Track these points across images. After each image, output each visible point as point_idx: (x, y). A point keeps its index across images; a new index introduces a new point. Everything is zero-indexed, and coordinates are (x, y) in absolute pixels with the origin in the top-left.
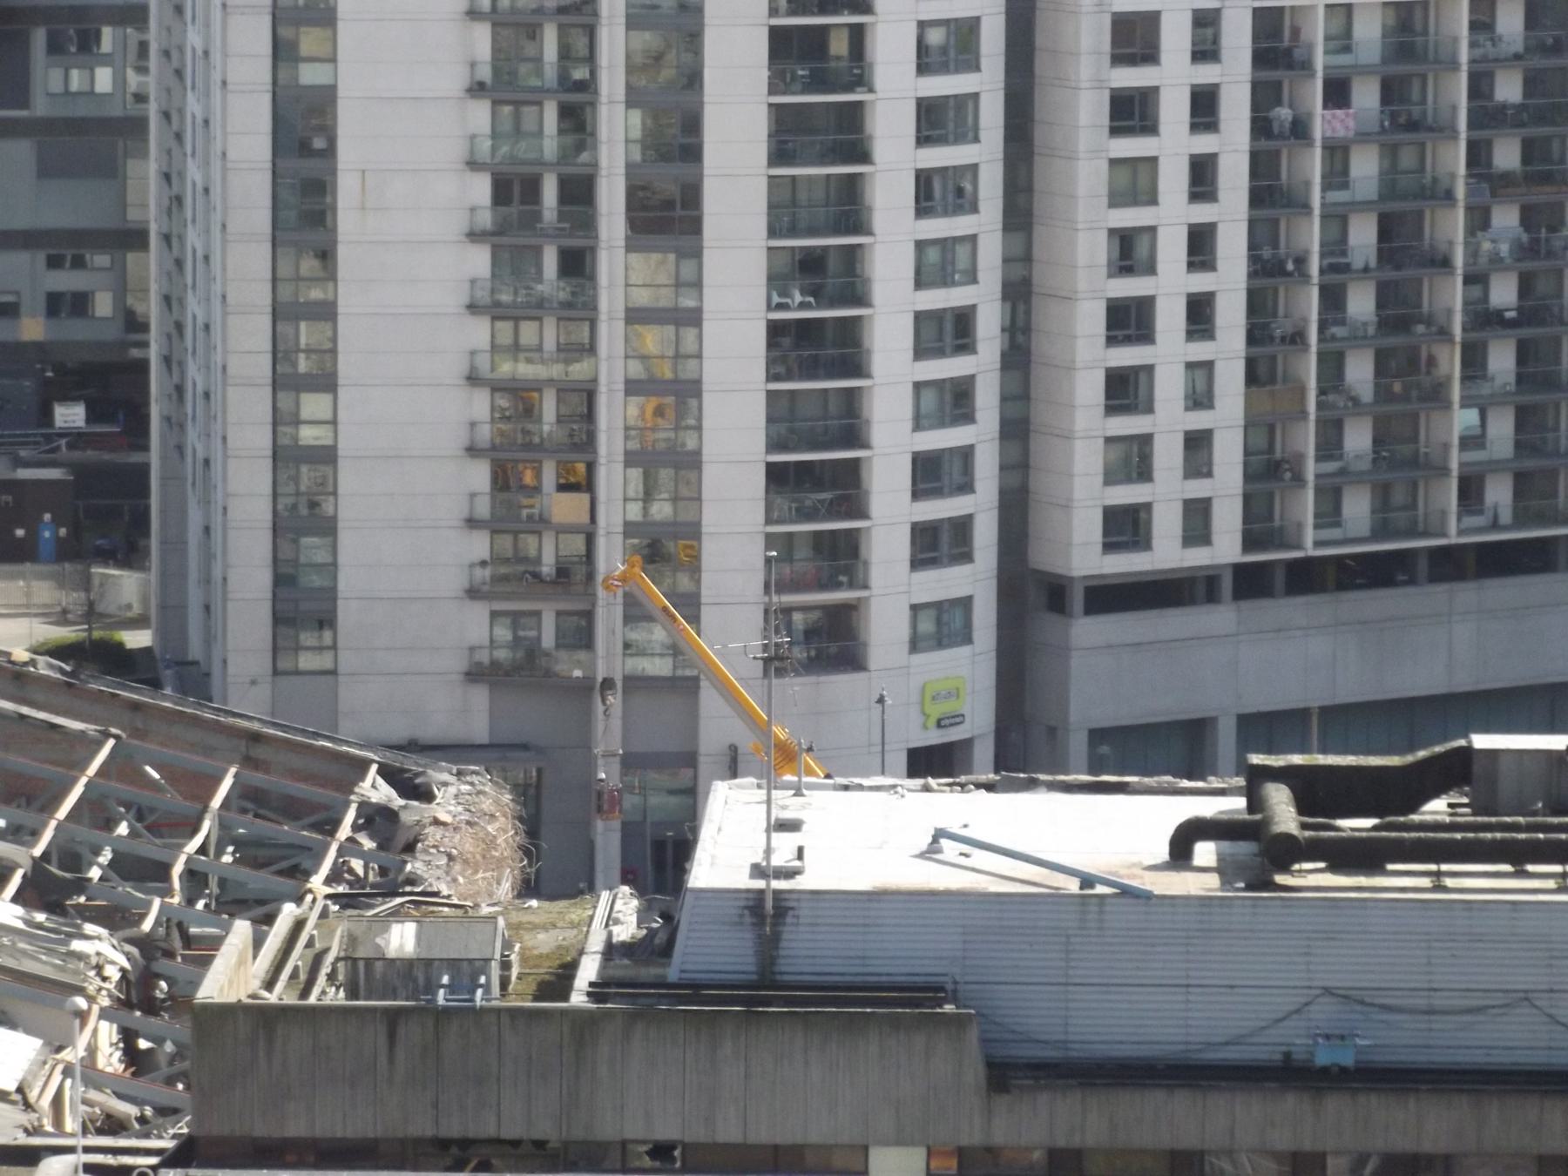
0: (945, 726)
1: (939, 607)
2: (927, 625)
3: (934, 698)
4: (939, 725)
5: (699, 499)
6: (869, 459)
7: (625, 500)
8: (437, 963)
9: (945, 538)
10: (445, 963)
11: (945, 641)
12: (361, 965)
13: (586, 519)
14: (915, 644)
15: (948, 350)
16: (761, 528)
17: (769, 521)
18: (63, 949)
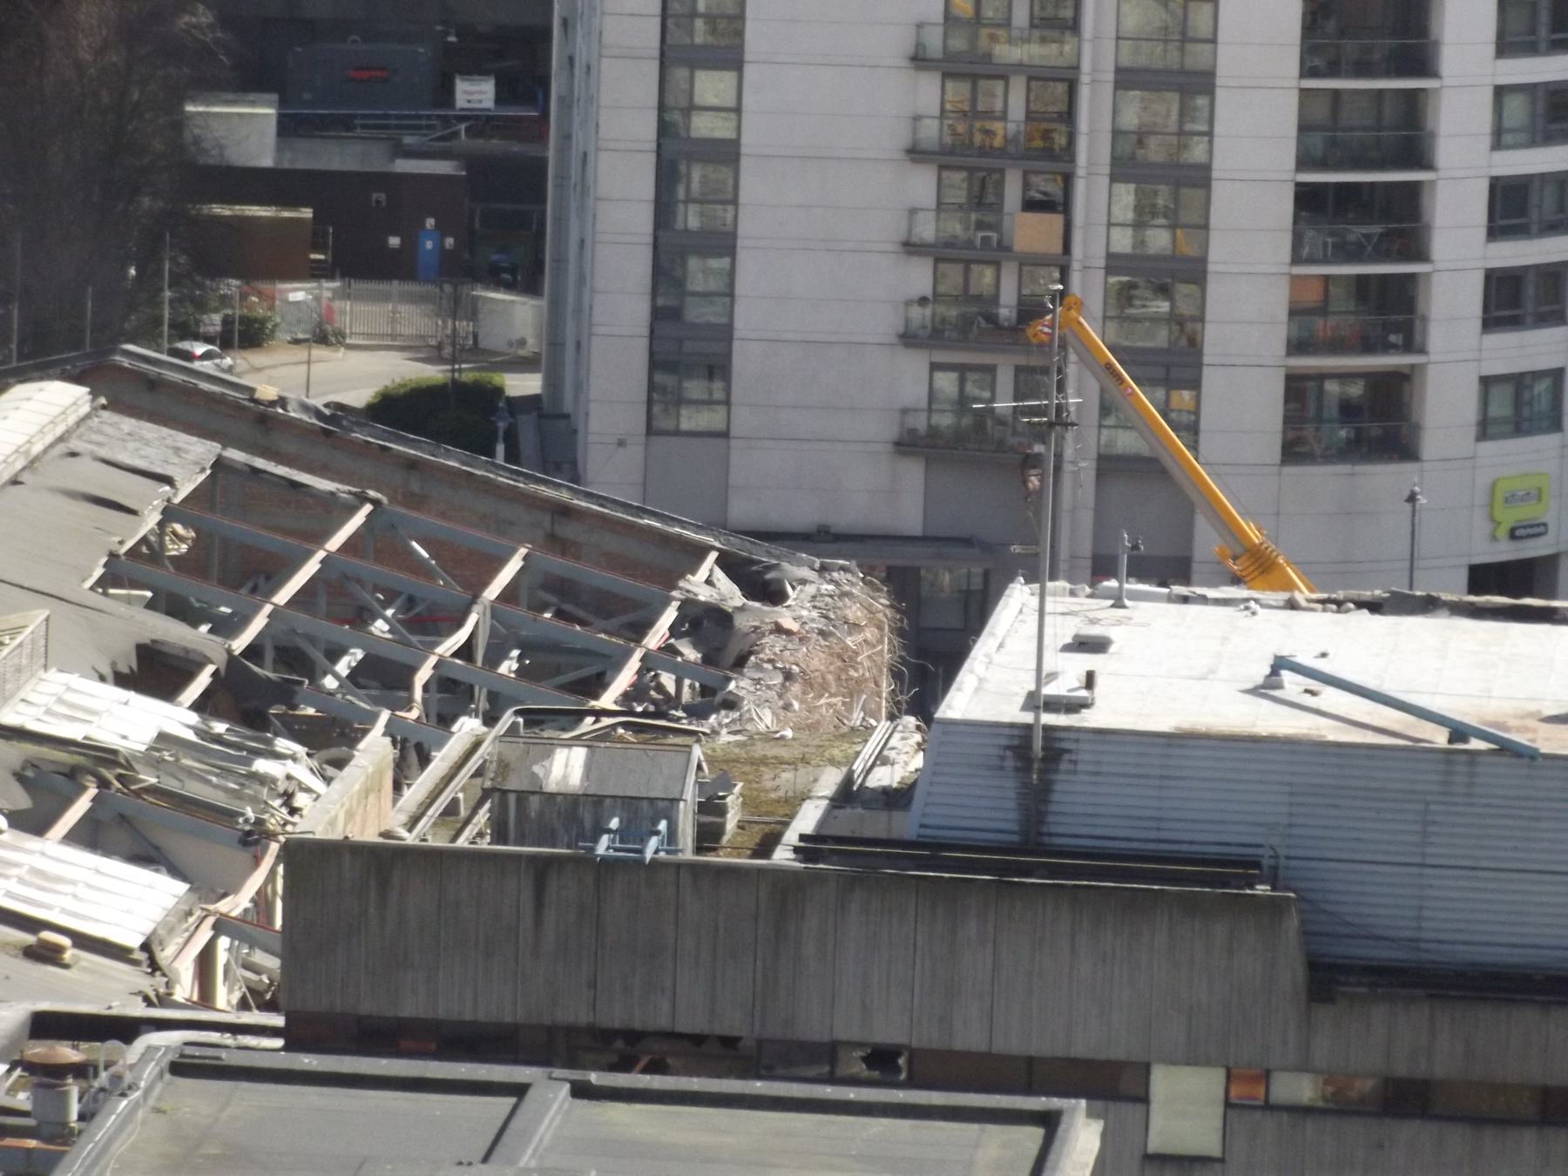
0: (1521, 538)
1: (1520, 382)
2: (1501, 406)
3: (1506, 500)
4: (1513, 535)
5: (1205, 227)
6: (1432, 183)
7: (1110, 225)
8: (608, 801)
9: (1530, 291)
10: (619, 801)
11: (1525, 426)
12: (512, 798)
13: (1057, 248)
14: (1486, 429)
15: (1543, 46)
16: (1286, 269)
17: (1296, 259)
18: (242, 770)
